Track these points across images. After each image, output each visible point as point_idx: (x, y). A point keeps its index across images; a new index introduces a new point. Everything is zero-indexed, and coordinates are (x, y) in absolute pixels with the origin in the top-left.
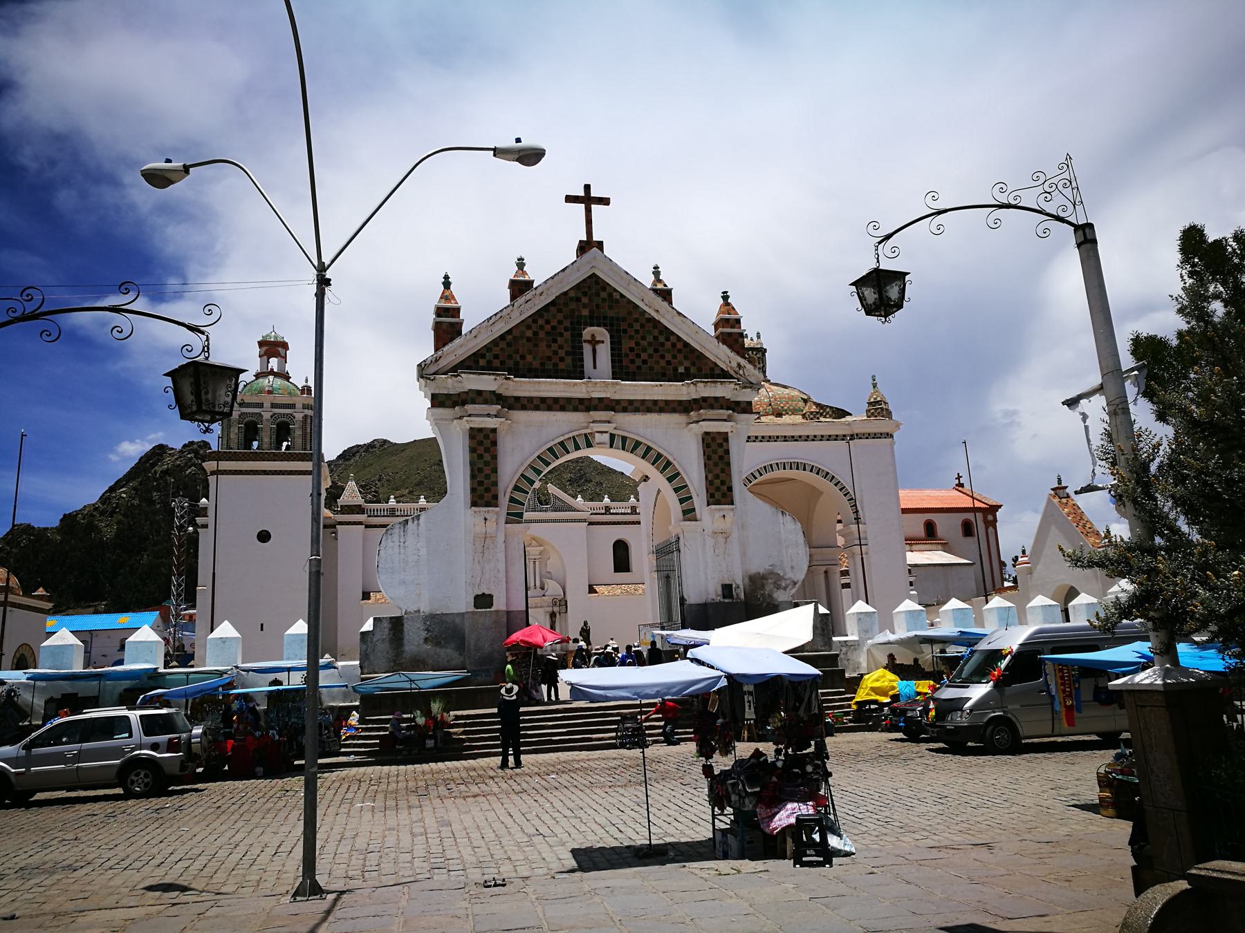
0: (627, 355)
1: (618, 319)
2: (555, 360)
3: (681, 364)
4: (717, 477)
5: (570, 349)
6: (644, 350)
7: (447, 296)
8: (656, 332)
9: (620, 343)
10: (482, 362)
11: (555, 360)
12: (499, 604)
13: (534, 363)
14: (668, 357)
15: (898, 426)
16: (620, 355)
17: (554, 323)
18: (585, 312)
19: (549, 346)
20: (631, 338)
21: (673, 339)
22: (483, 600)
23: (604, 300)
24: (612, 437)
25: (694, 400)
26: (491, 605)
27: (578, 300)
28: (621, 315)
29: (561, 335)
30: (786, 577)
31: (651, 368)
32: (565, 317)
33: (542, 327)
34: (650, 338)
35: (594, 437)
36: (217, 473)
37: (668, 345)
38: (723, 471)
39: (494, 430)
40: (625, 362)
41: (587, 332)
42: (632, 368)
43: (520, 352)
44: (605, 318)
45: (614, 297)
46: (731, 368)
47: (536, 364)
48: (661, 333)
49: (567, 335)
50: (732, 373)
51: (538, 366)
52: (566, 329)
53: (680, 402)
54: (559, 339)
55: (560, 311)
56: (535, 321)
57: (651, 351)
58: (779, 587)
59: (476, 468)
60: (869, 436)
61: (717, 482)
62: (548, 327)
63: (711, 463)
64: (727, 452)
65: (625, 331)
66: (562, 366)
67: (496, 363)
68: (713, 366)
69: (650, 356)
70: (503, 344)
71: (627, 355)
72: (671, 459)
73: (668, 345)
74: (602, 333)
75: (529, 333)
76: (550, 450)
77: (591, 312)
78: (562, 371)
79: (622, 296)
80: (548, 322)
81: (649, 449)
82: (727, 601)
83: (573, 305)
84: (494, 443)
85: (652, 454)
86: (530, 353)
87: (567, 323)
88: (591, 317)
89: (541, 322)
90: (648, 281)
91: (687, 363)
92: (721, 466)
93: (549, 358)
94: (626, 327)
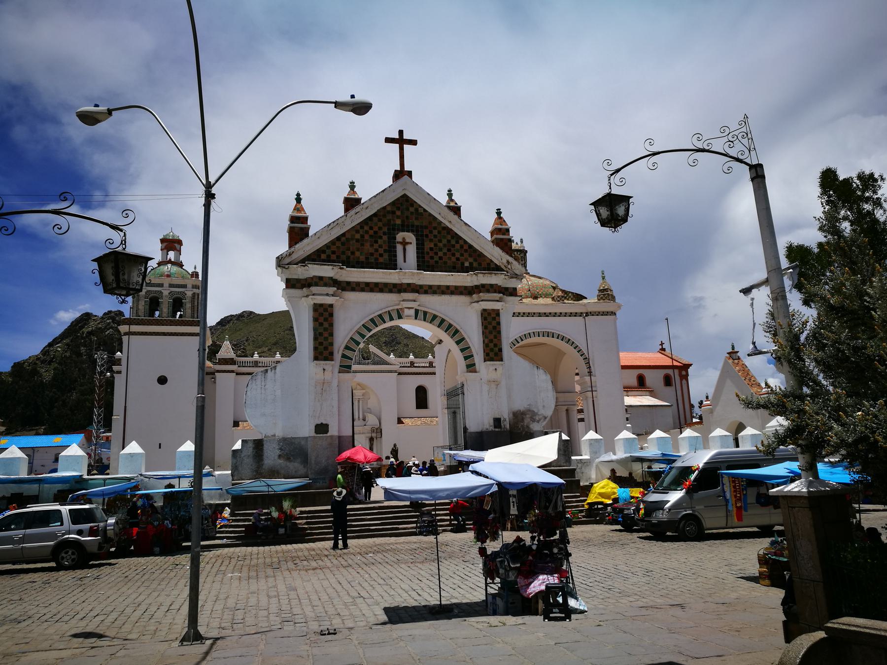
0: (428, 253)
1: (422, 227)
2: (376, 255)
3: (467, 260)
4: (491, 341)
5: (387, 248)
6: (441, 250)
7: (298, 207)
8: (449, 237)
9: (423, 244)
10: (323, 256)
11: (376, 255)
12: (333, 431)
13: (361, 257)
15: (619, 307)
16: (423, 253)
17: (376, 229)
18: (398, 222)
19: (372, 246)
20: (431, 240)
21: (461, 242)
22: (322, 428)
23: (412, 213)
24: (417, 311)
25: (476, 286)
26: (327, 432)
27: (393, 213)
28: (424, 225)
29: (381, 238)
30: (539, 413)
31: (445, 263)
32: (384, 225)
33: (367, 232)
34: (444, 241)
35: (404, 312)
36: (129, 333)
37: (458, 246)
38: (495, 337)
39: (331, 306)
40: (427, 258)
41: (400, 236)
42: (432, 262)
43: (351, 249)
44: (413, 226)
45: (419, 211)
46: (502, 263)
47: (362, 258)
48: (453, 237)
49: (385, 238)
50: (503, 267)
51: (364, 260)
52: (384, 234)
53: (466, 288)
54: (379, 241)
55: (380, 220)
56: (362, 227)
57: (445, 250)
58: (534, 420)
59: (317, 333)
60: (598, 314)
61: (491, 345)
62: (371, 232)
63: (487, 331)
64: (499, 324)
65: (427, 236)
66: (381, 260)
67: (334, 257)
68: (489, 262)
69: (445, 254)
70: (338, 244)
71: (428, 253)
72: (459, 328)
73: (458, 246)
74: (410, 237)
75: (358, 236)
76: (372, 320)
77: (403, 221)
78: (381, 263)
79: (425, 210)
80: (371, 228)
81: (443, 321)
82: (497, 430)
83: (389, 217)
84: (331, 315)
85: (445, 325)
86: (358, 250)
87: (385, 229)
88: (403, 225)
89: (366, 228)
90: (444, 200)
91: (471, 260)
92: (494, 333)
93: (372, 254)
94: (428, 233)
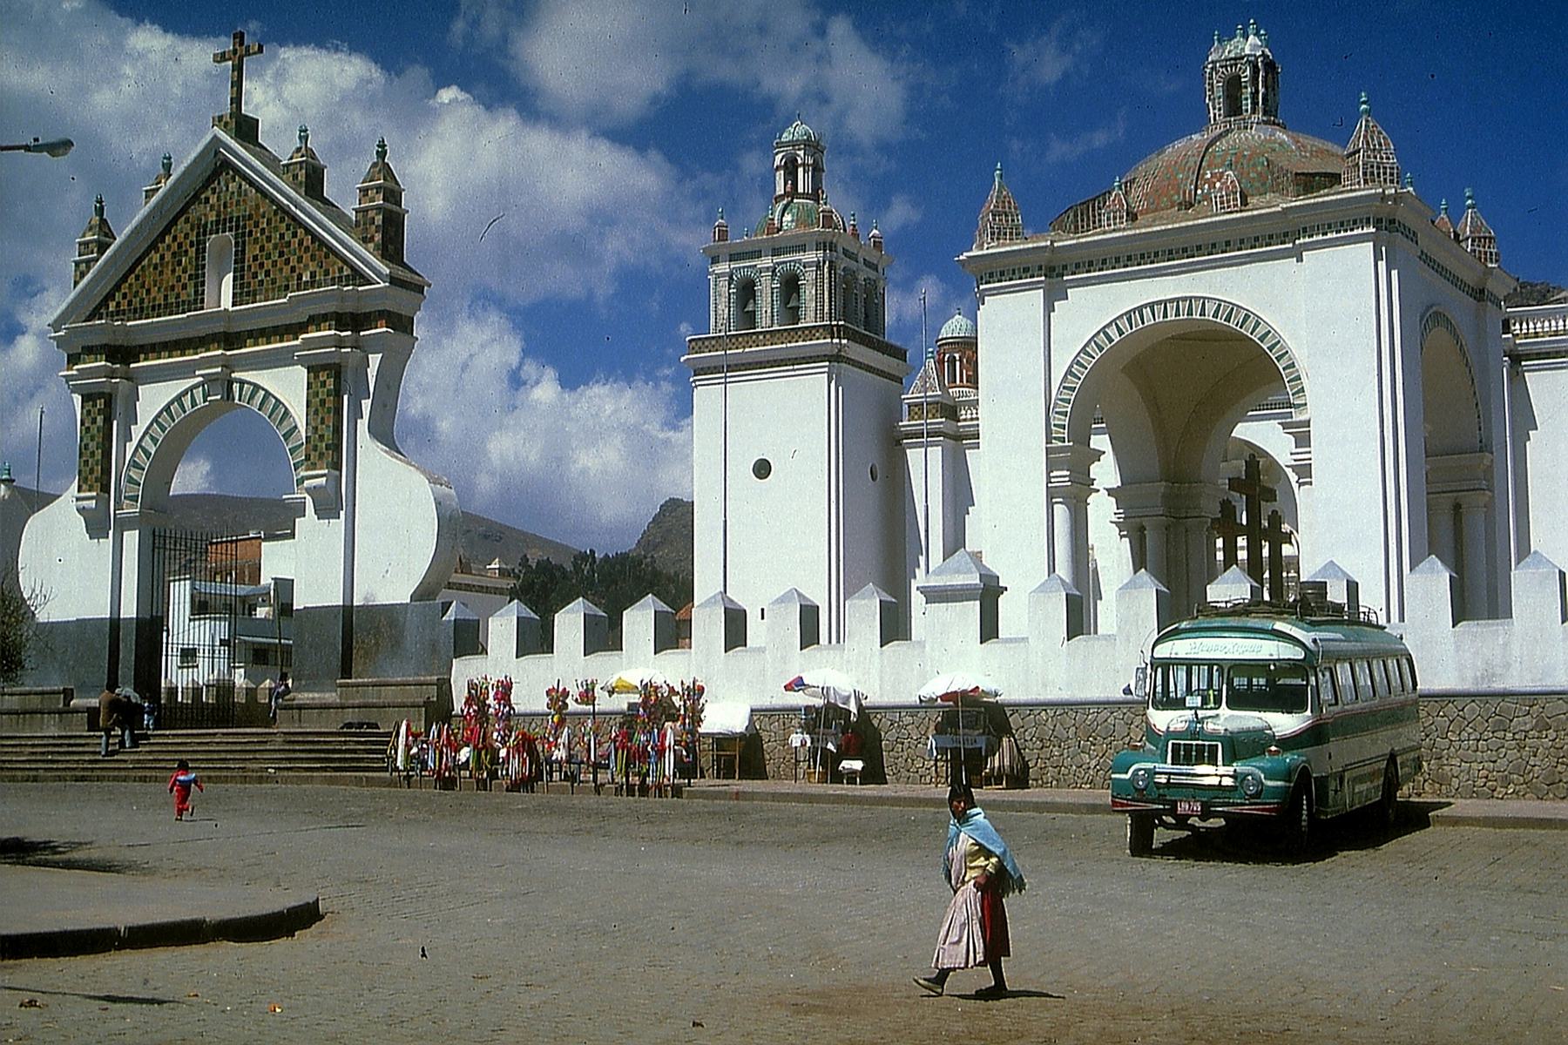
14: (293, 261)
18: (212, 217)
31: (274, 282)
42: (254, 284)
57: (275, 256)
62: (175, 246)
77: (218, 215)
88: (218, 222)
